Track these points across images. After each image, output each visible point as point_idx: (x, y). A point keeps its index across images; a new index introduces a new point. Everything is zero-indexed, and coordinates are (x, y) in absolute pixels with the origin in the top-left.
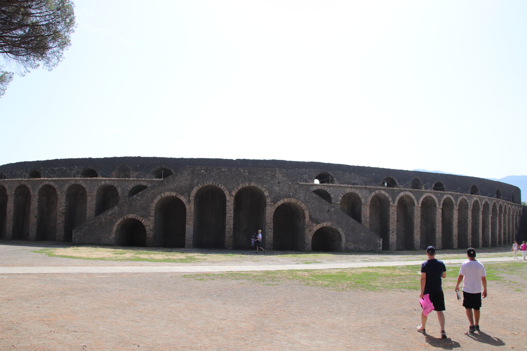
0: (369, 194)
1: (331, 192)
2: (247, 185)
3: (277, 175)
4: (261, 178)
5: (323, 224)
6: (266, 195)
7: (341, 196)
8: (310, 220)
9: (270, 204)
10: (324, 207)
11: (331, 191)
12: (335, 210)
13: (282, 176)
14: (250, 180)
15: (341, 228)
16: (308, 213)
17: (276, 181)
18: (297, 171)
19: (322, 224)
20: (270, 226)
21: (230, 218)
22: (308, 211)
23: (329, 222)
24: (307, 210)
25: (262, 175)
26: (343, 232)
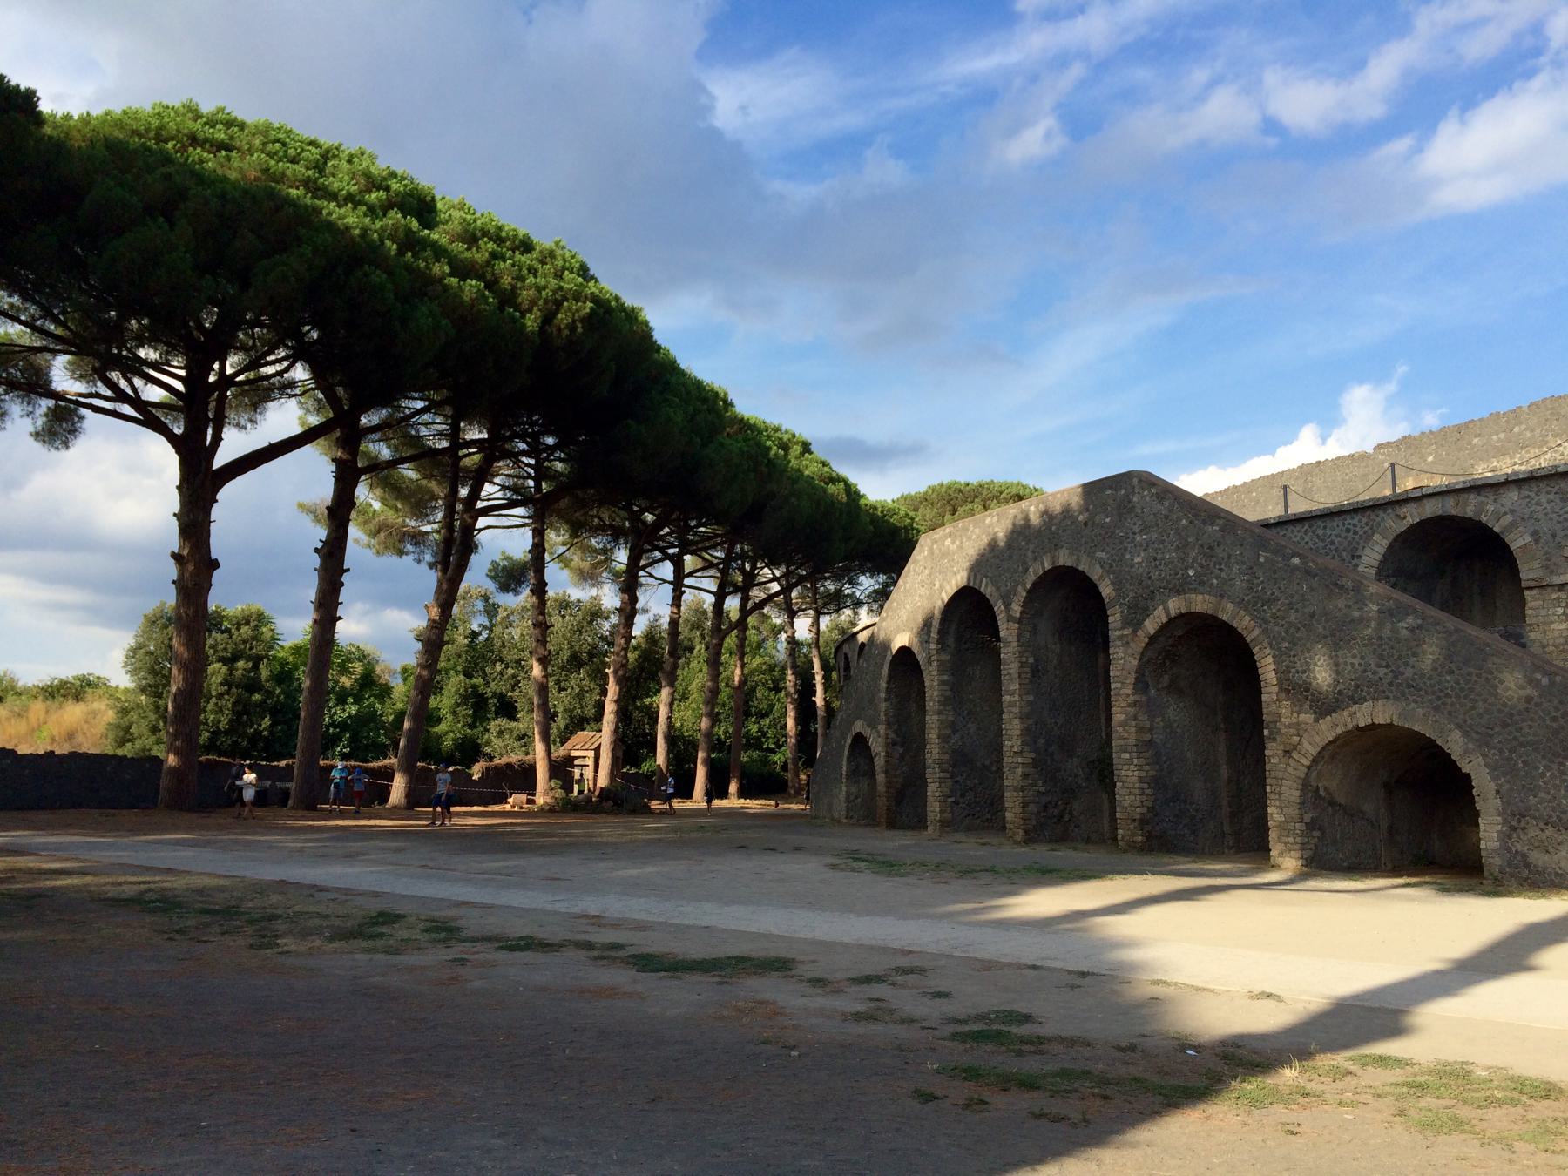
2: (1048, 566)
5: (1352, 715)
8: (1283, 695)
9: (1121, 632)
11: (1512, 511)
17: (1135, 524)
19: (1346, 713)
20: (1126, 735)
22: (1271, 647)
23: (1388, 698)
26: (1484, 756)
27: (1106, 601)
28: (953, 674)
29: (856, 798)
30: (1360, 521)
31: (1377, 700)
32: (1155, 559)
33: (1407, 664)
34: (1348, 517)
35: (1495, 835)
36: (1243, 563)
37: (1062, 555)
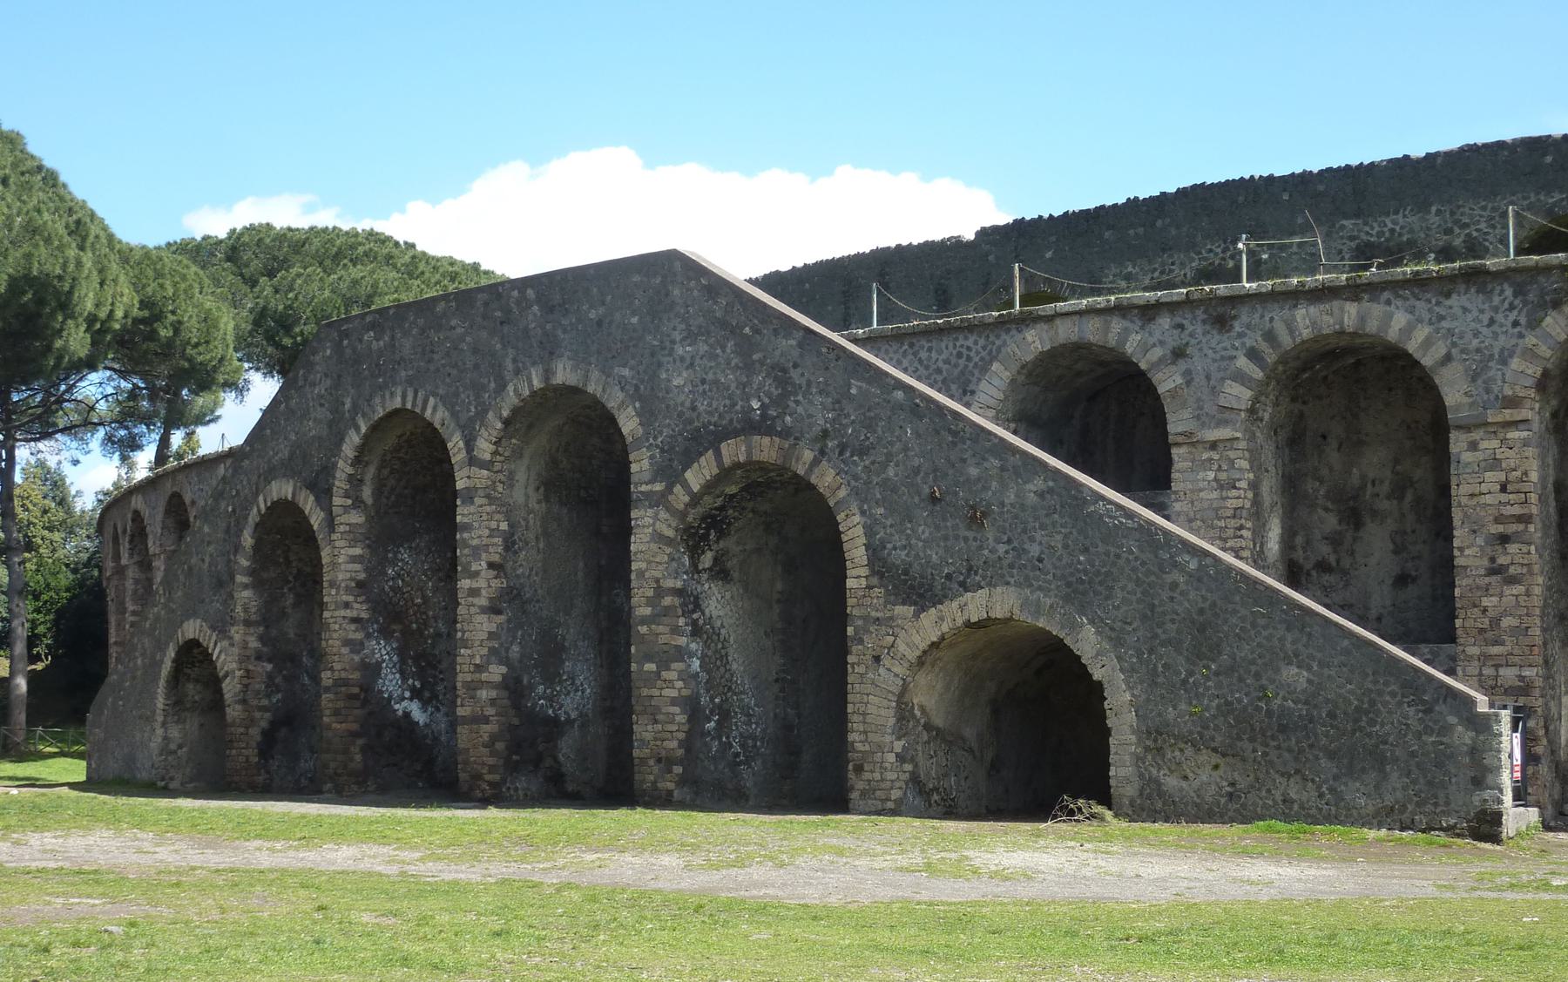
0: (1516, 324)
1: (1157, 353)
2: (537, 383)
4: (599, 323)
5: (961, 608)
6: (625, 431)
7: (1240, 377)
8: (875, 581)
10: (974, 472)
11: (1162, 343)
12: (1051, 491)
14: (549, 351)
15: (1098, 633)
16: (859, 531)
17: (674, 329)
18: (1352, 238)
19: (955, 604)
21: (473, 605)
22: (863, 513)
23: (1008, 583)
24: (856, 510)
25: (603, 303)
26: (1119, 658)
27: (629, 439)
28: (369, 546)
29: (180, 747)
30: (976, 343)
33: (1032, 539)
34: (961, 337)
35: (1127, 757)
36: (827, 395)
37: (560, 366)
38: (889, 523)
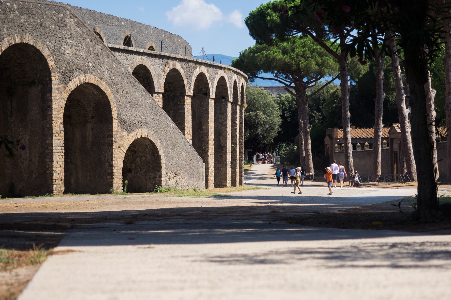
2: (18, 41)
3: (67, 21)
9: (58, 86)
13: (75, 22)
15: (160, 142)
17: (66, 34)
27: (51, 69)
31: (142, 128)
32: (76, 54)
38: (122, 107)
